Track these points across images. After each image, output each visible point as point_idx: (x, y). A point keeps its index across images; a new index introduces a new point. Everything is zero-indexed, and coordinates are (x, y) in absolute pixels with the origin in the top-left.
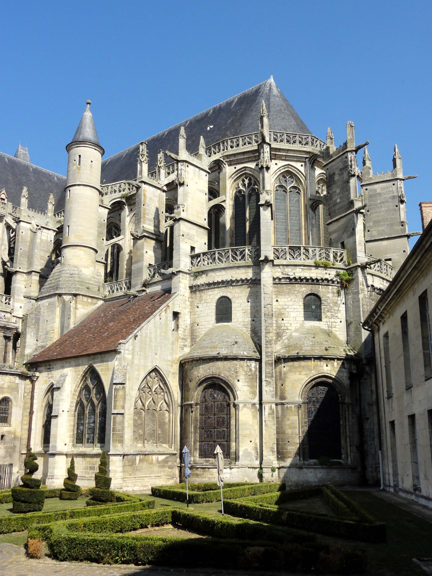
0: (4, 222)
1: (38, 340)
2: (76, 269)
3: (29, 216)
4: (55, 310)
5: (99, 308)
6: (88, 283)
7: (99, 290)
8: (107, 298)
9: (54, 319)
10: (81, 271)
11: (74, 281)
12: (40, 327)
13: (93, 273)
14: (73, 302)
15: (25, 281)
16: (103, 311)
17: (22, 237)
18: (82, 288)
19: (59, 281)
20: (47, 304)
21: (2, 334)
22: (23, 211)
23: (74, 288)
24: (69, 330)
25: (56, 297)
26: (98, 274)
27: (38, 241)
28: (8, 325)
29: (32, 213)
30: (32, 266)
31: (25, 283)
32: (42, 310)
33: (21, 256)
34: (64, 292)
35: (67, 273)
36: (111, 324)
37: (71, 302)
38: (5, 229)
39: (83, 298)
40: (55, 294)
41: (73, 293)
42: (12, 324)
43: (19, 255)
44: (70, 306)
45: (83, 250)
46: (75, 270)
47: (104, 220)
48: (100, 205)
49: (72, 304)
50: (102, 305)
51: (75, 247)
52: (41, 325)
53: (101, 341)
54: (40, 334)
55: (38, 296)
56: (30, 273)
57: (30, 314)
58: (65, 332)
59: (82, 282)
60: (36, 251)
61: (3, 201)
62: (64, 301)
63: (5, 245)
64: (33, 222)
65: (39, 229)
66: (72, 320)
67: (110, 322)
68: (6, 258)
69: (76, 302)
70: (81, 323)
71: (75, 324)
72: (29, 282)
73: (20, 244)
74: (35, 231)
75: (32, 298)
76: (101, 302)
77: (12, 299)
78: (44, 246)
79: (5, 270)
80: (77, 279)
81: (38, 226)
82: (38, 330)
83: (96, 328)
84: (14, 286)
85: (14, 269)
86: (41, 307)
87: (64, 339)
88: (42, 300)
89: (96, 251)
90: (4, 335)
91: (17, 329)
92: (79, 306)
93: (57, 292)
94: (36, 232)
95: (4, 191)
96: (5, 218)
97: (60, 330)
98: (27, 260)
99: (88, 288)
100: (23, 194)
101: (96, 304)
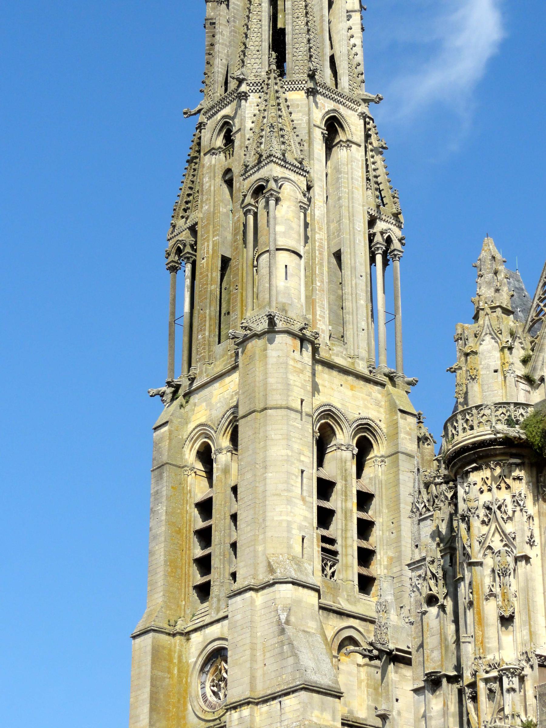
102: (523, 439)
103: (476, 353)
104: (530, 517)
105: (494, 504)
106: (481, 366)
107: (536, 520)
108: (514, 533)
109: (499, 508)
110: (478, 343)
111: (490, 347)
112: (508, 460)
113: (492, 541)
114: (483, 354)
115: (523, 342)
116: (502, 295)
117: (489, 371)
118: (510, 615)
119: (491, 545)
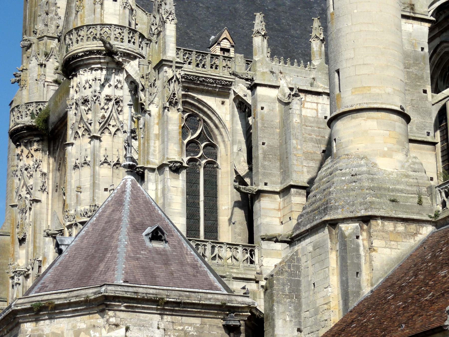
0: (232, 96)
1: (302, 328)
2: (363, 162)
3: (272, 72)
4: (327, 258)
5: (424, 242)
6: (393, 190)
7: (420, 203)
8: (440, 217)
9: (326, 278)
10: (375, 165)
11: (361, 188)
12: (303, 300)
13: (403, 167)
14: (365, 234)
15: (279, 210)
16: (431, 248)
17: (262, 119)
18: (379, 203)
19: (330, 193)
20: (310, 248)
21: (221, 323)
22: (258, 65)
23: (361, 204)
24: (361, 298)
25: (326, 230)
26: (416, 167)
27: (296, 120)
28: (231, 301)
29: (277, 66)
30: (288, 176)
31: (279, 214)
32: (303, 263)
33: (264, 158)
34: (341, 217)
35: (344, 175)
36: (442, 273)
37: (358, 237)
38: (236, 110)
39: (383, 226)
40: (324, 224)
41: (359, 215)
42: (240, 299)
43: (261, 156)
44: (358, 246)
45: (373, 118)
46: (361, 166)
47: (422, 49)
48: (404, 16)
49: (360, 241)
50: (432, 235)
51: (355, 115)
52: (303, 295)
53: (416, 313)
54: (304, 315)
55: (293, 233)
56: (285, 191)
57: (277, 273)
58: (353, 304)
59: (380, 189)
60: (294, 142)
61: (226, 54)
62: (342, 235)
63: (240, 142)
64: (282, 83)
65: (296, 95)
66: (365, 276)
67: (442, 268)
68: (243, 169)
69: (370, 236)
70: (387, 280)
71: (372, 285)
72: (287, 211)
73: (260, 134)
74: (286, 100)
75: (279, 239)
76: (428, 230)
77: (256, 251)
78: (313, 131)
79: (244, 195)
80: (366, 184)
81: (291, 89)
82: (298, 307)
83: (410, 285)
84: (259, 222)
85: (255, 188)
86: (300, 256)
87: (349, 321)
88: (300, 240)
89: (407, 119)
90: (224, 323)
91: (251, 308)
92: (376, 243)
93: (327, 218)
94: (288, 104)
95: (226, 34)
96: (233, 88)
97: (341, 302)
98: (278, 164)
99: (393, 201)
100: (256, 28)
101: (416, 234)
102: (35, 126)
103: (26, 70)
104: (44, 174)
105: (23, 168)
106: (29, 78)
107: (51, 175)
108: (32, 185)
109: (26, 169)
110: (29, 63)
111: (35, 64)
112: (33, 139)
113: (22, 191)
114: (31, 70)
115: (58, 58)
116: (52, 27)
117: (33, 80)
118: (22, 238)
119: (21, 194)
